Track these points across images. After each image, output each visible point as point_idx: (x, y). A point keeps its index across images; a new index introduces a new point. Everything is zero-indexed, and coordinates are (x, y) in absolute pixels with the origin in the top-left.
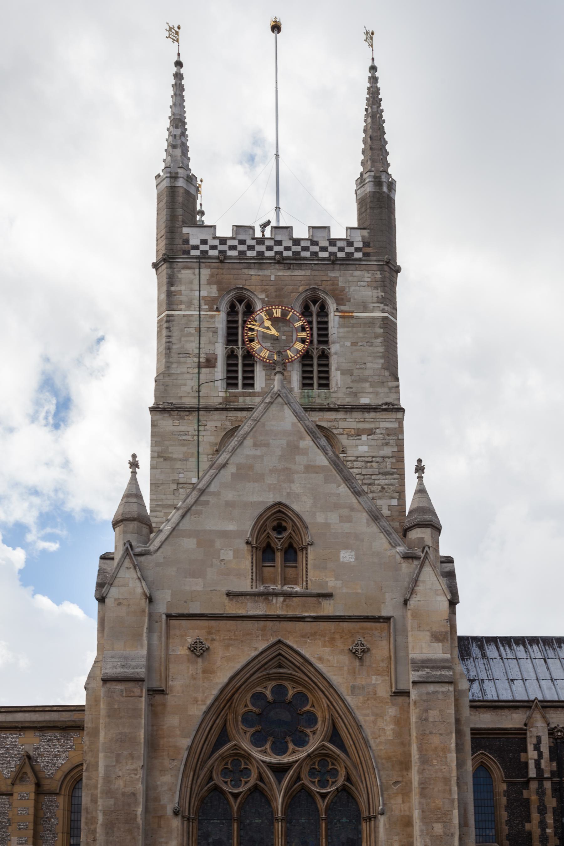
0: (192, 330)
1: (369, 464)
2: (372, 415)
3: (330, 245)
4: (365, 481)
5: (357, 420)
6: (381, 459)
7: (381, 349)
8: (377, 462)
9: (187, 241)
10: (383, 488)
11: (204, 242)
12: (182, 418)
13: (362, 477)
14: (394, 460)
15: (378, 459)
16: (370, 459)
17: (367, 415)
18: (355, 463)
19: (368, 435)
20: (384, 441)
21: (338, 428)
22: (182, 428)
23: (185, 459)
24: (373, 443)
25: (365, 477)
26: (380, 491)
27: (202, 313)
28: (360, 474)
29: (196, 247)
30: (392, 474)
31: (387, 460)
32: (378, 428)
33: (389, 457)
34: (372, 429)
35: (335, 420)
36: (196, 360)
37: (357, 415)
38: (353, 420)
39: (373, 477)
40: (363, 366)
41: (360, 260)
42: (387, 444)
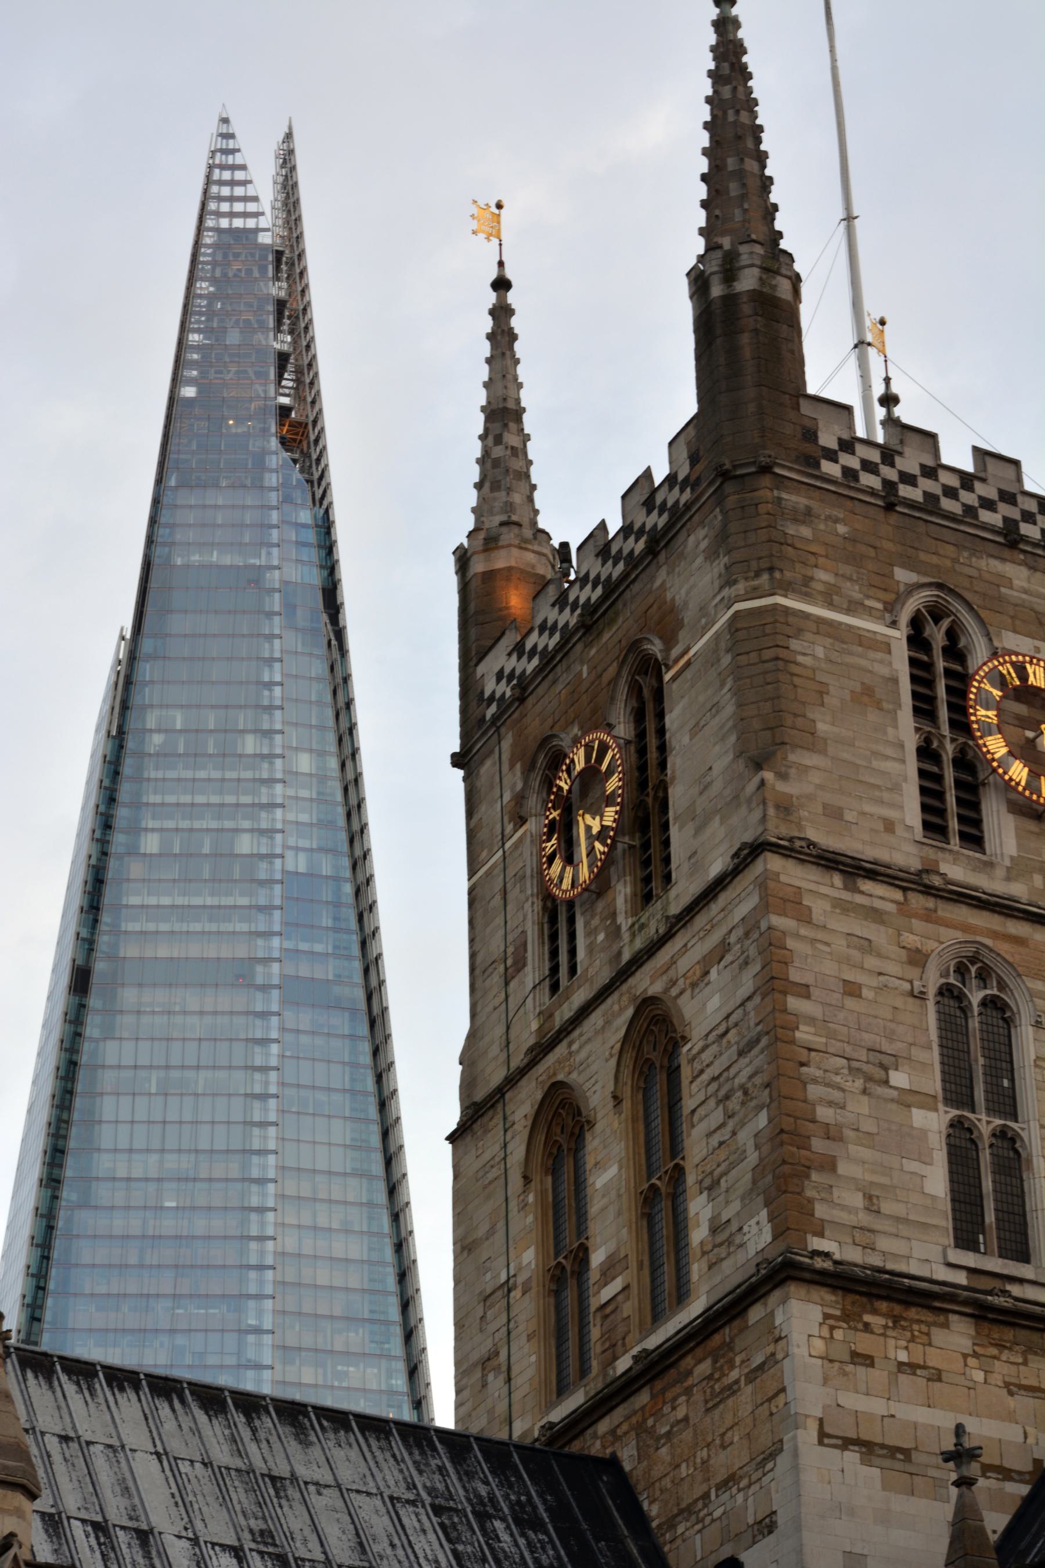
0: (497, 900)
1: (725, 1041)
2: (723, 899)
3: (649, 512)
4: (722, 1093)
5: (702, 934)
6: (740, 1011)
7: (730, 709)
8: (736, 1025)
9: (482, 693)
10: (746, 1093)
11: (500, 675)
12: (487, 1131)
13: (714, 1086)
14: (757, 999)
15: (733, 1019)
16: (722, 1029)
17: (715, 908)
18: (703, 1056)
19: (719, 963)
20: (741, 960)
21: (677, 980)
22: (487, 1156)
23: (491, 1232)
24: (727, 974)
25: (722, 1079)
26: (743, 1103)
27: (508, 845)
28: (714, 1079)
29: (492, 698)
30: (758, 1041)
31: (750, 1005)
32: (731, 931)
33: (749, 998)
34: (723, 941)
35: (673, 962)
36: (502, 968)
37: (700, 921)
38: (696, 938)
39: (732, 1071)
40: (708, 779)
41: (688, 506)
42: (746, 963)
